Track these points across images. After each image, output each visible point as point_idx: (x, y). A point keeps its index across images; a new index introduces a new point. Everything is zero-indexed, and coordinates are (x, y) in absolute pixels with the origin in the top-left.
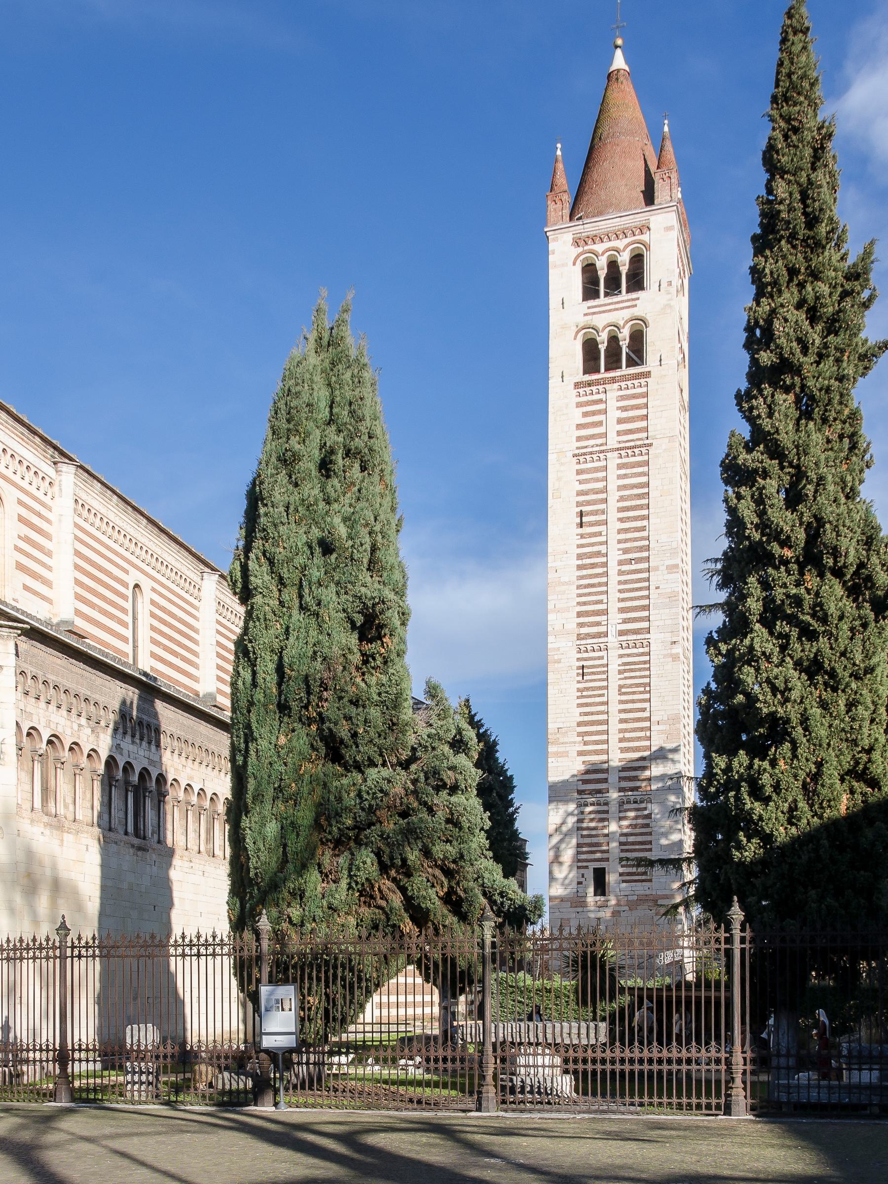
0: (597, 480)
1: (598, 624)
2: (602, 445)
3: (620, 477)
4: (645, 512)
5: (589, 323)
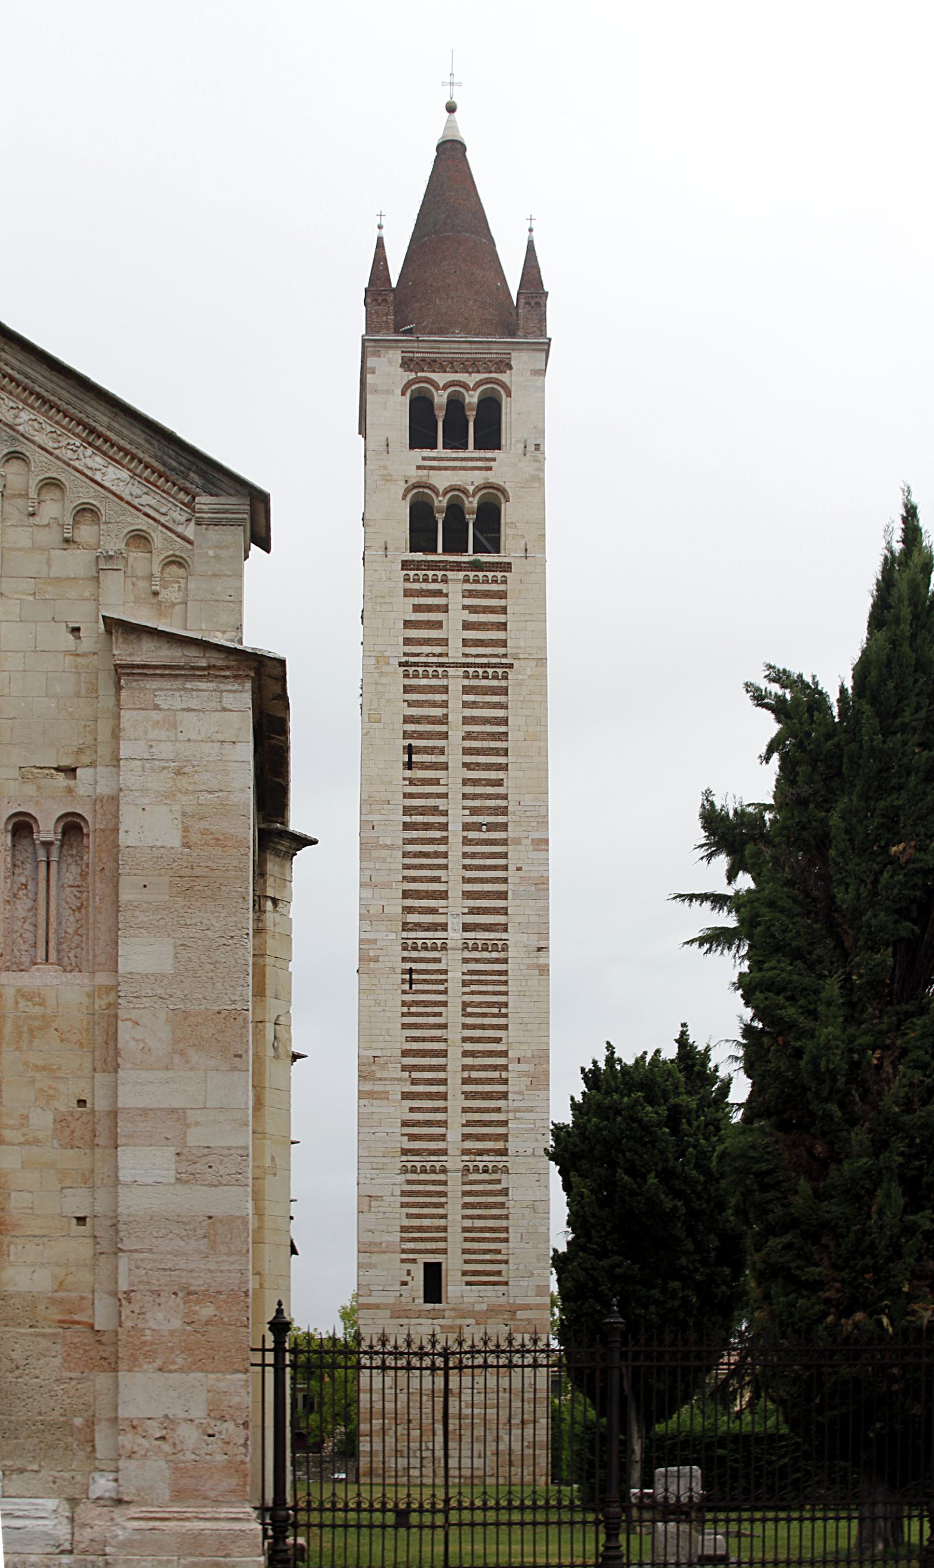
0: (434, 704)
1: (434, 911)
2: (440, 655)
3: (465, 705)
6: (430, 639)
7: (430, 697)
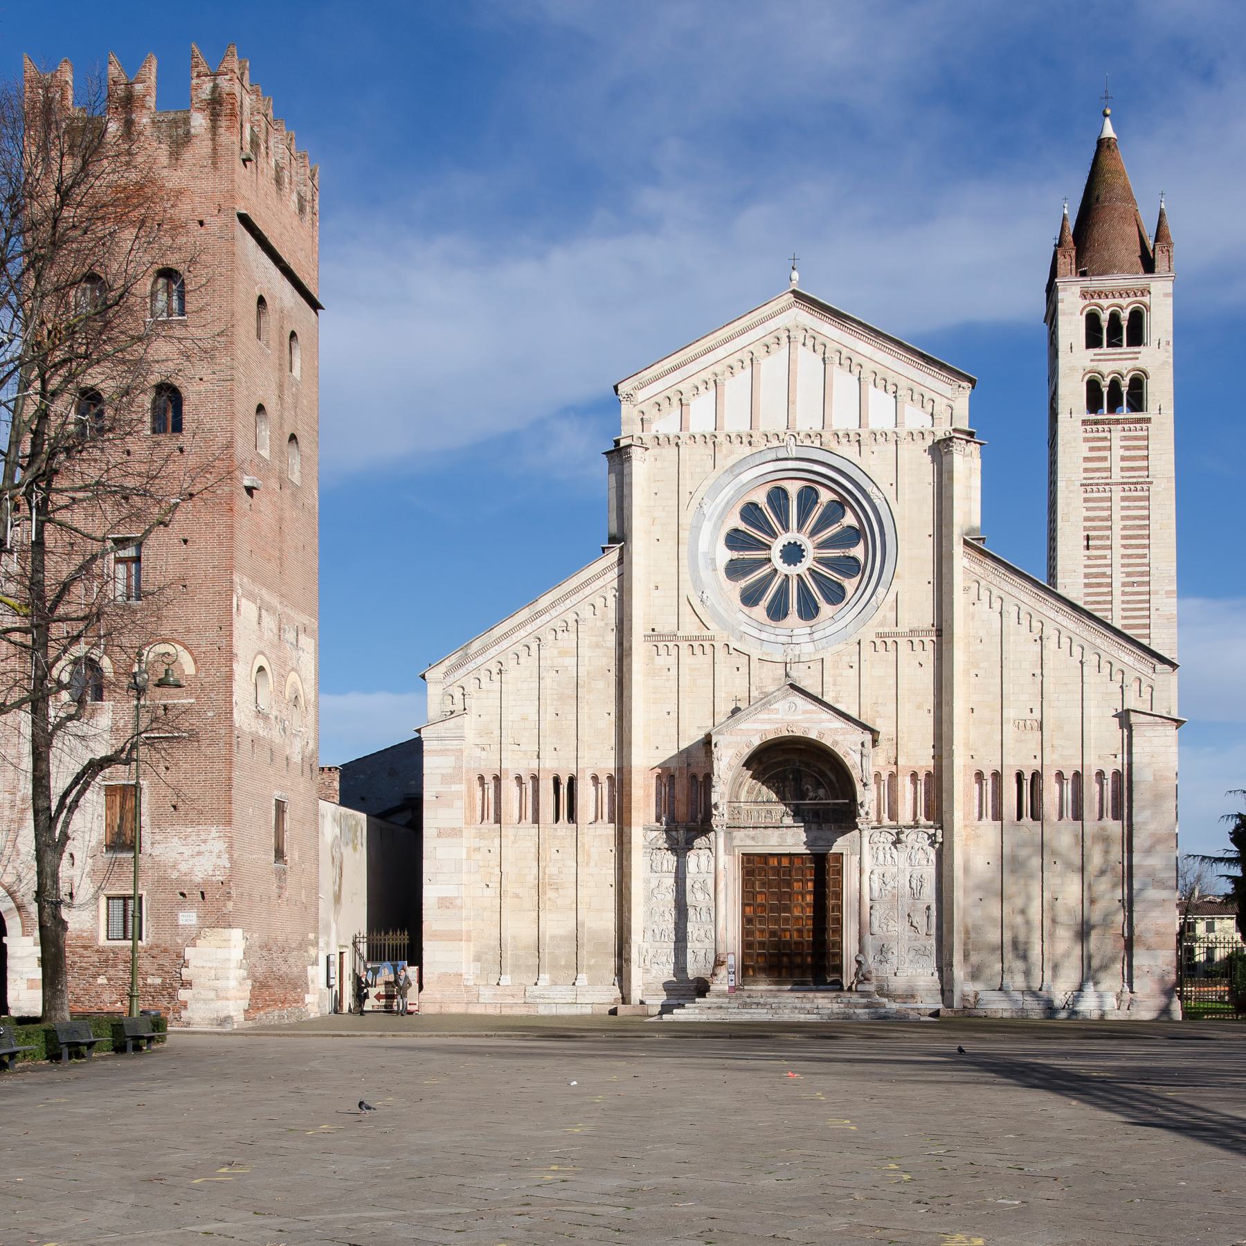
0: (1102, 509)
2: (1106, 478)
3: (1123, 508)
4: (1146, 542)
5: (1096, 368)
6: (1099, 468)
7: (1100, 504)
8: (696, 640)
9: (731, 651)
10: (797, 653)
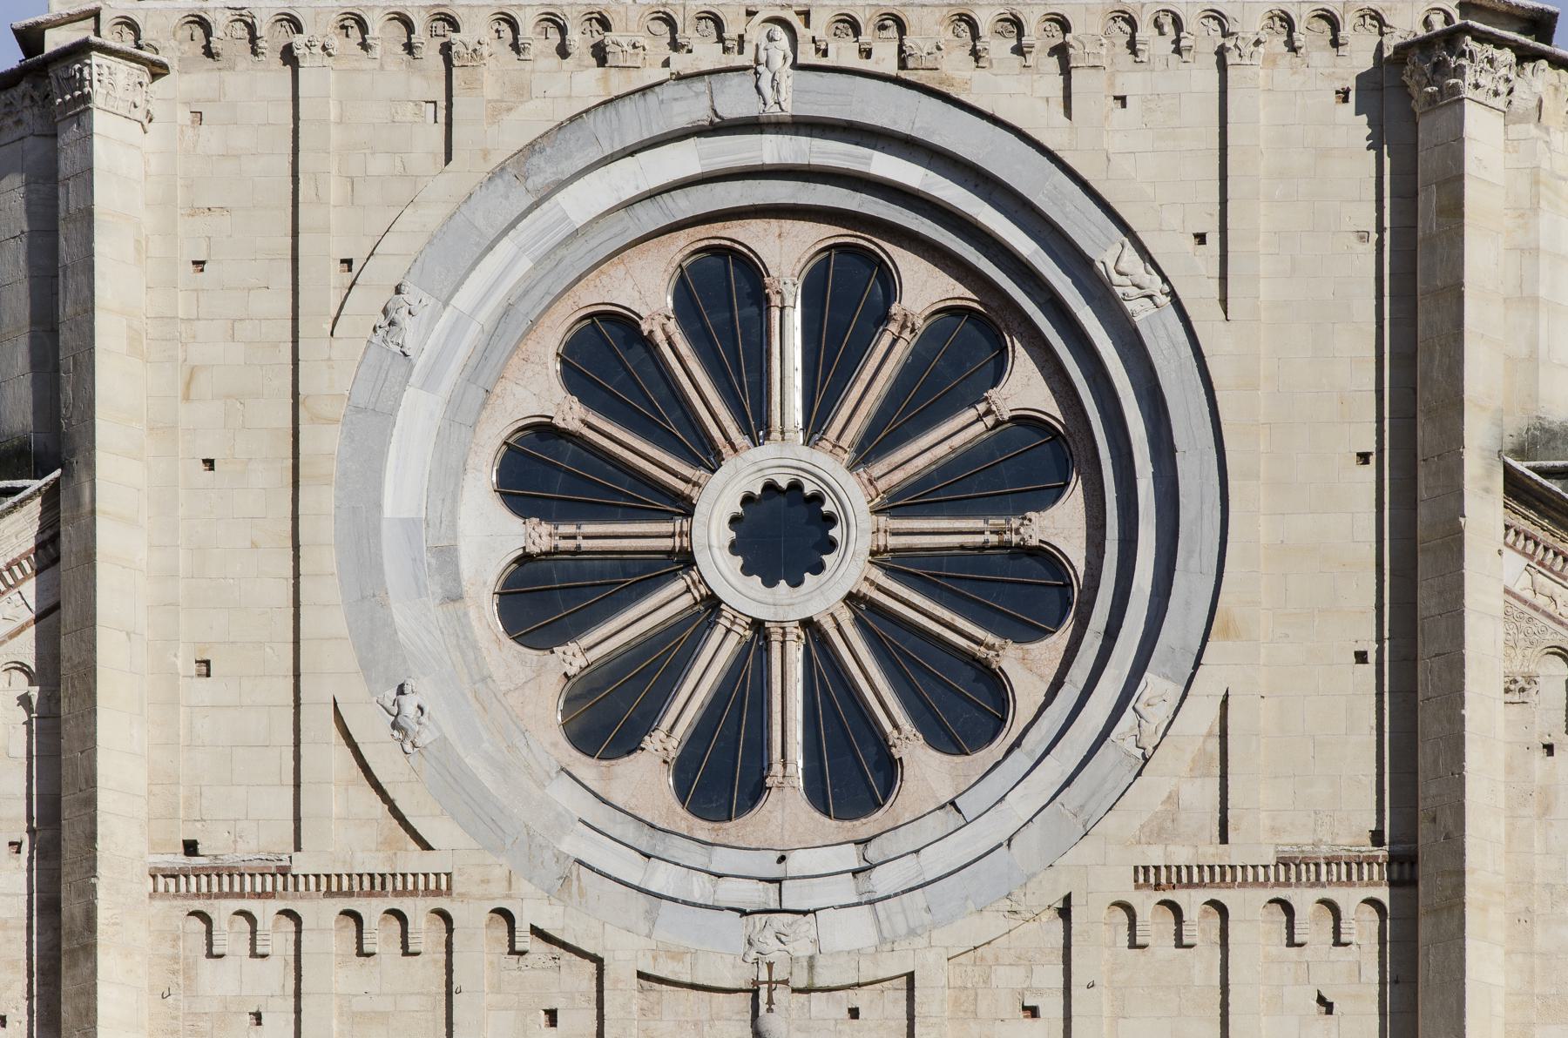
8: (371, 893)
9: (524, 940)
10: (802, 949)
